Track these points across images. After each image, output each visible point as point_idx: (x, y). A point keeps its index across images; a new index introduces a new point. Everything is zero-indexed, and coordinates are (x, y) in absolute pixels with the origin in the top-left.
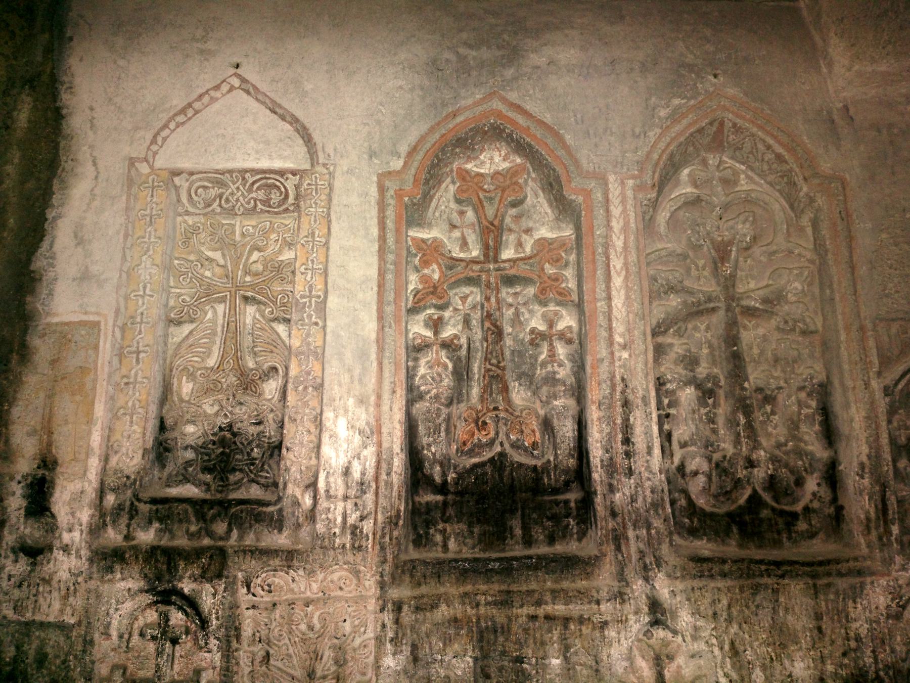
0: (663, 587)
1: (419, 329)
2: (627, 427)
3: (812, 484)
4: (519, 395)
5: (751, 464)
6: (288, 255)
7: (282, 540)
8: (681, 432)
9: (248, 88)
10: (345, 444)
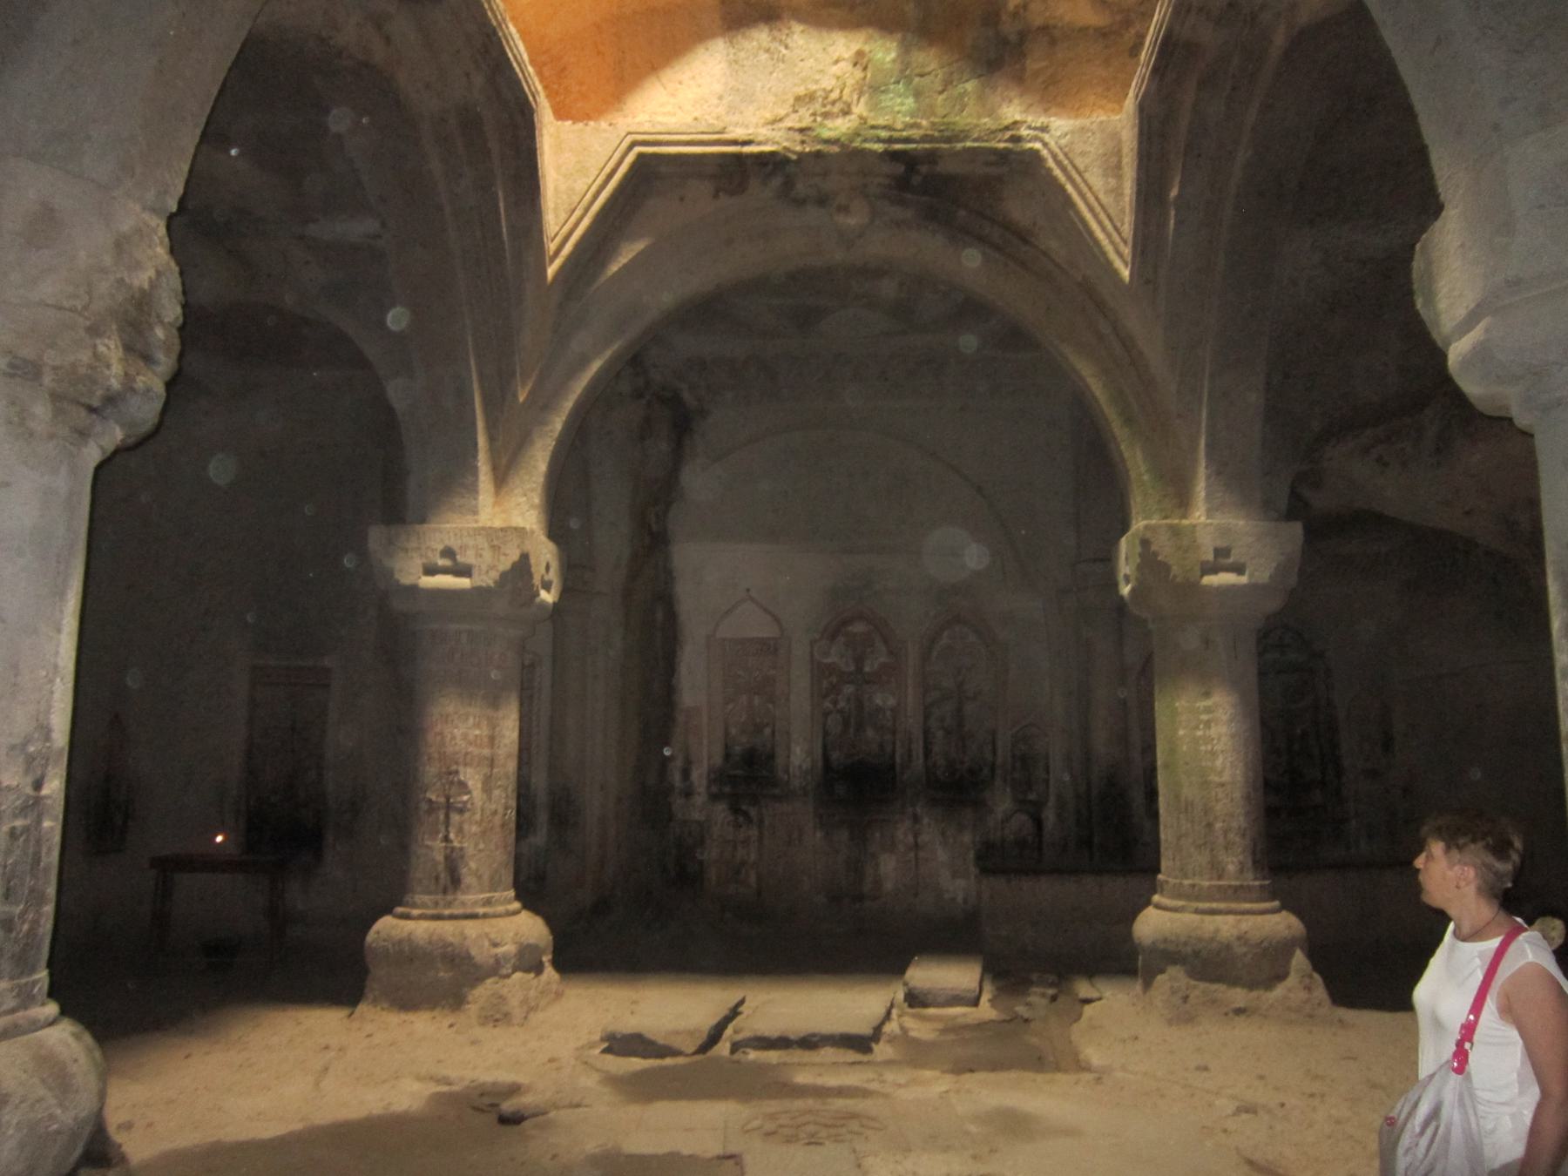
0: (919, 810)
1: (828, 704)
2: (910, 750)
3: (986, 771)
4: (870, 733)
5: (962, 763)
6: (773, 672)
7: (777, 791)
8: (936, 749)
9: (752, 599)
10: (799, 756)
